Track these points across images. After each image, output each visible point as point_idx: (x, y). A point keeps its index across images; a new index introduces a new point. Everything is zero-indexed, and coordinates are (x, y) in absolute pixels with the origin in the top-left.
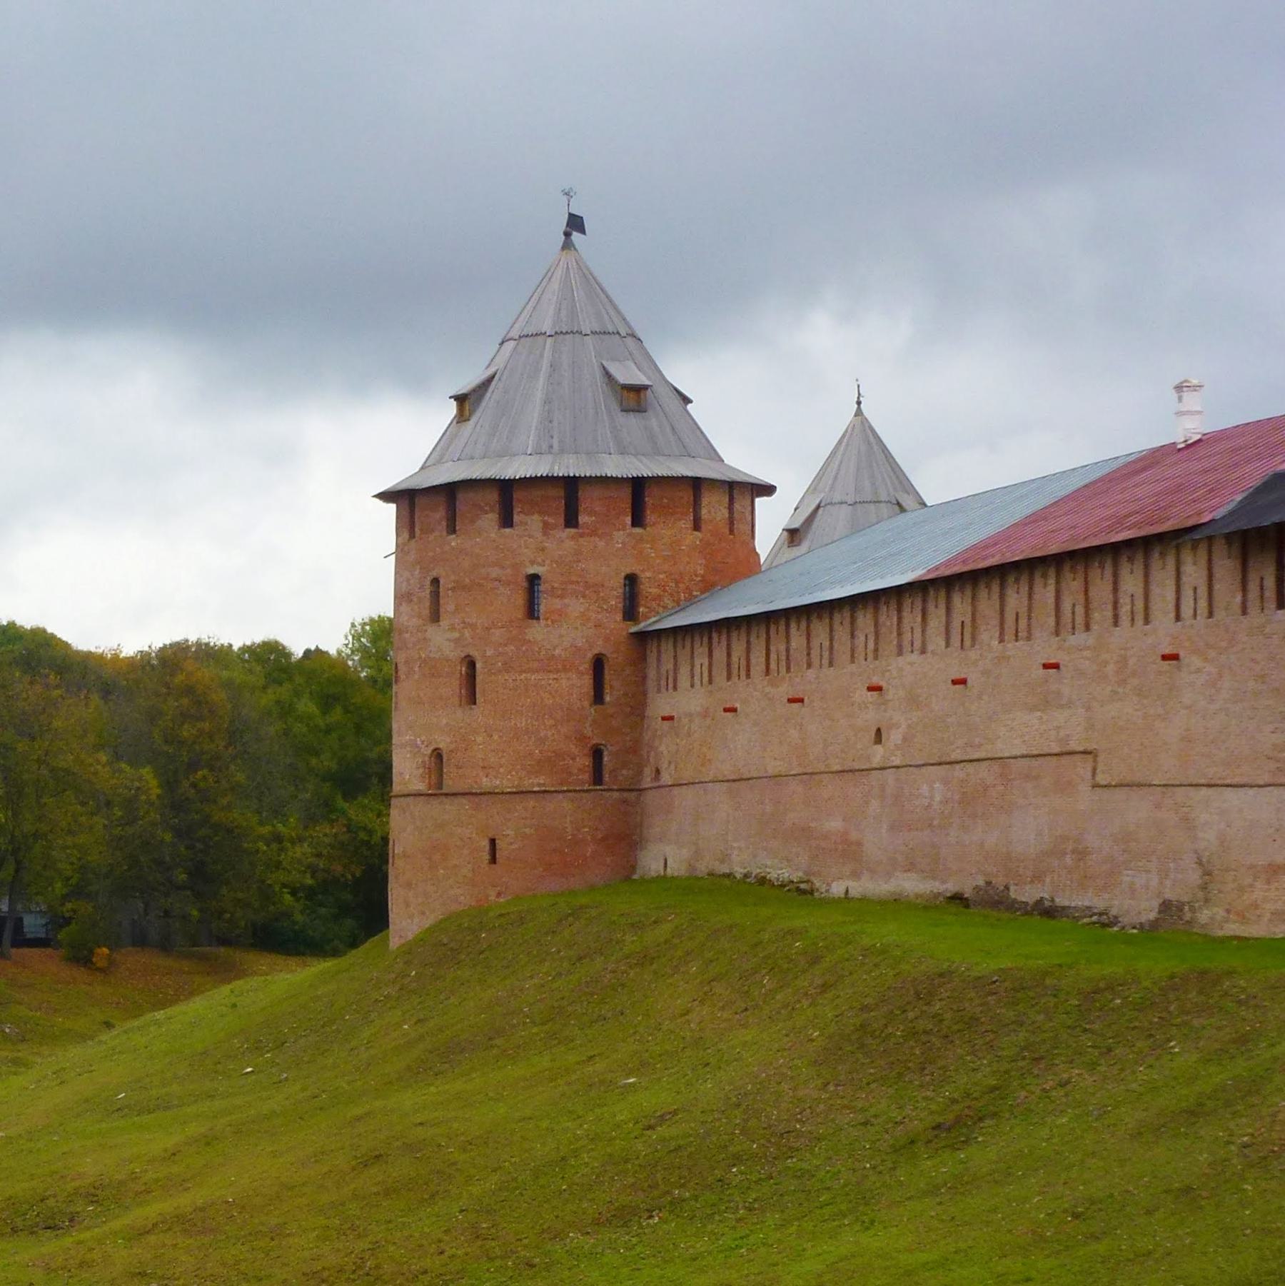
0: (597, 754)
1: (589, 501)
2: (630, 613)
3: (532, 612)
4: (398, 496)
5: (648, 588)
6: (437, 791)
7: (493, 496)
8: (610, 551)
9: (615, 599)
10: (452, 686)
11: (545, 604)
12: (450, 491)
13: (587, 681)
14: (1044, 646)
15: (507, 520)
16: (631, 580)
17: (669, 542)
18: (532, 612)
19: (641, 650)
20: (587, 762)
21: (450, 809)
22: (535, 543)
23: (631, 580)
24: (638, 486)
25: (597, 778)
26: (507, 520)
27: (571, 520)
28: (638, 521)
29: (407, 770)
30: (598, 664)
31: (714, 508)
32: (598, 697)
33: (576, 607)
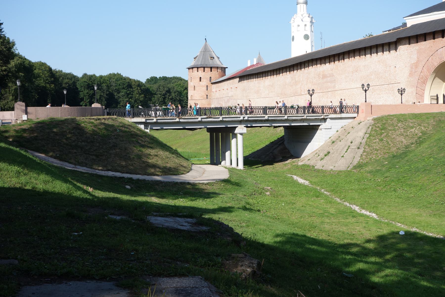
2: (210, 81)
3: (200, 81)
6: (192, 100)
10: (193, 89)
13: (206, 88)
15: (198, 71)
16: (211, 77)
18: (200, 81)
20: (206, 96)
23: (211, 77)
25: (207, 98)
26: (198, 71)
28: (211, 71)
30: (207, 86)
32: (207, 90)
33: (205, 80)
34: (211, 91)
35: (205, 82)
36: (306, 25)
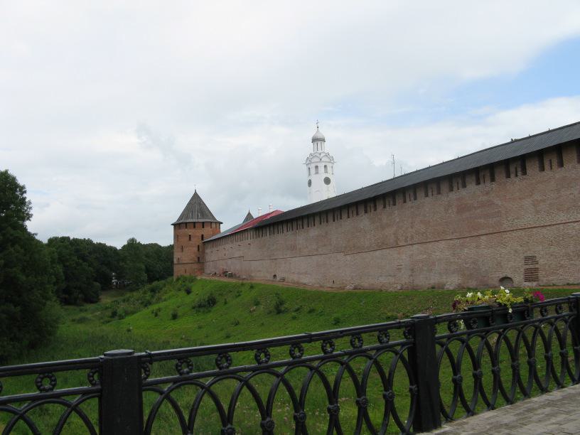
0: (199, 258)
1: (196, 225)
2: (202, 239)
4: (174, 225)
5: (205, 236)
7: (185, 225)
8: (198, 232)
9: (201, 238)
10: (180, 250)
11: (192, 238)
12: (180, 224)
14: (239, 243)
16: (202, 236)
17: (207, 231)
19: (205, 244)
21: (180, 266)
22: (190, 231)
23: (202, 236)
24: (203, 223)
25: (199, 260)
27: (195, 227)
29: (175, 261)
30: (198, 246)
31: (214, 225)
32: (198, 250)
34: (204, 252)
35: (196, 241)
36: (325, 166)
